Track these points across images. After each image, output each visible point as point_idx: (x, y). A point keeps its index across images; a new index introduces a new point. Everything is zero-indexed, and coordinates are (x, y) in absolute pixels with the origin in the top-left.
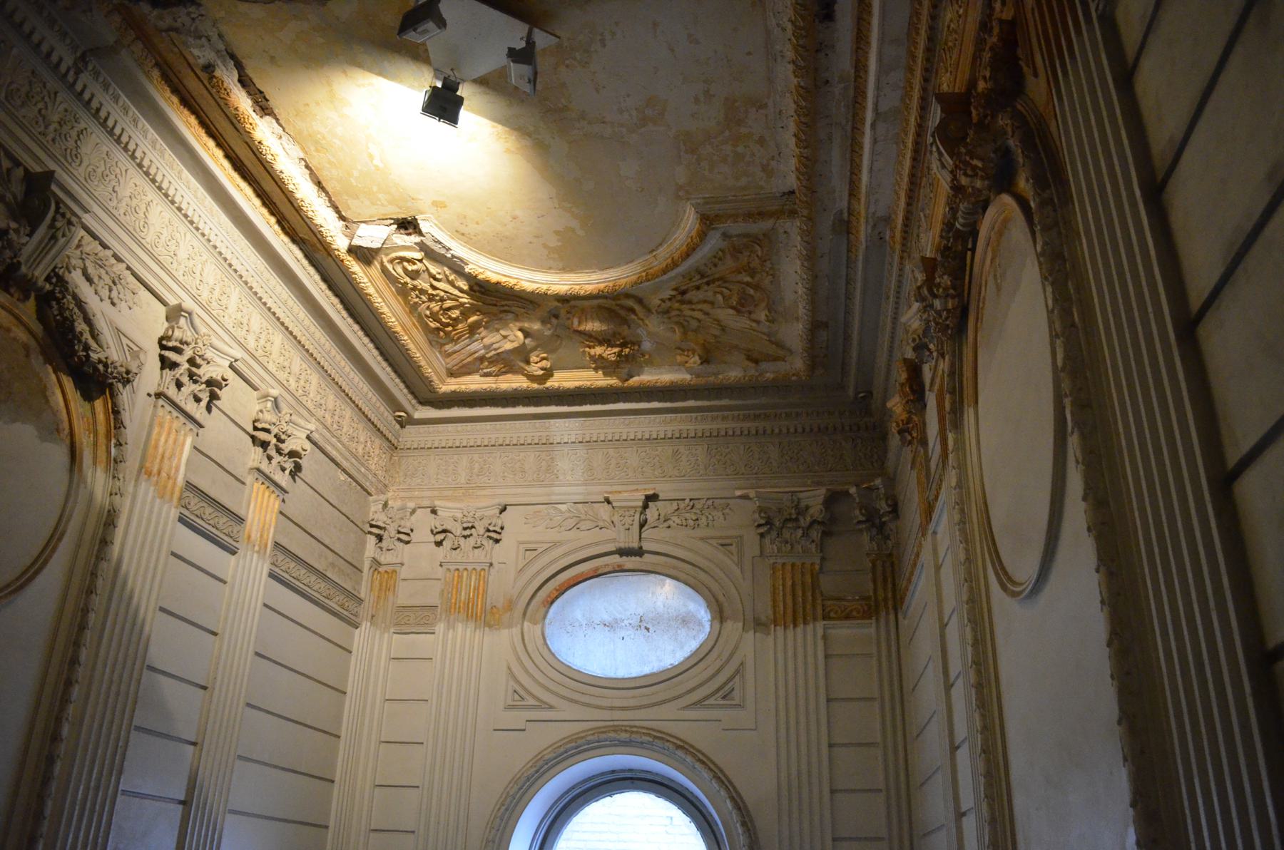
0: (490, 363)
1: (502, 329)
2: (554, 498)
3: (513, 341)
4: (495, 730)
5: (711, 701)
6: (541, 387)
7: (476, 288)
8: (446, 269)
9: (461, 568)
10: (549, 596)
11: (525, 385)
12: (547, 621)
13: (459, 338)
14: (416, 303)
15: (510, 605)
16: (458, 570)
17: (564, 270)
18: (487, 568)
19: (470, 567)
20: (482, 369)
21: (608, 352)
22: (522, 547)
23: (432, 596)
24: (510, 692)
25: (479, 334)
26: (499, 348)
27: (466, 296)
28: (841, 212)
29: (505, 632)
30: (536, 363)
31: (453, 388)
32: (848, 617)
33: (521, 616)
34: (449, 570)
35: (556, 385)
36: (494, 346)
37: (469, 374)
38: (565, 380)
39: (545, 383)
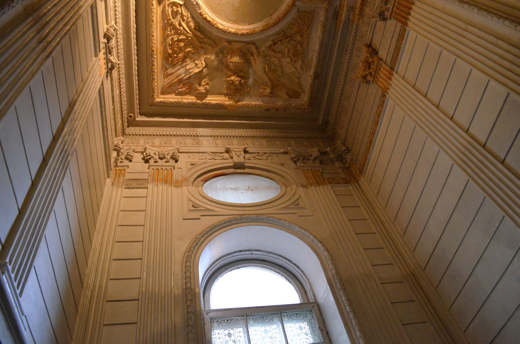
0: (183, 85)
1: (197, 60)
2: (202, 150)
3: (198, 68)
4: (184, 219)
5: (291, 206)
6: (201, 102)
7: (197, 28)
8: (189, 14)
9: (159, 168)
10: (204, 179)
11: (194, 101)
12: (204, 188)
13: (177, 63)
14: (168, 34)
15: (186, 180)
16: (158, 169)
17: (235, 22)
18: (172, 169)
19: (164, 168)
20: (179, 89)
21: (236, 79)
22: (189, 164)
23: (146, 176)
24: (191, 206)
25: (186, 62)
26: (191, 72)
27: (191, 33)
28: (336, 7)
29: (184, 188)
30: (204, 86)
31: (161, 100)
32: (339, 183)
33: (192, 182)
34: (153, 169)
35: (208, 101)
36: (190, 71)
37: (170, 93)
38: (212, 99)
39: (203, 101)
